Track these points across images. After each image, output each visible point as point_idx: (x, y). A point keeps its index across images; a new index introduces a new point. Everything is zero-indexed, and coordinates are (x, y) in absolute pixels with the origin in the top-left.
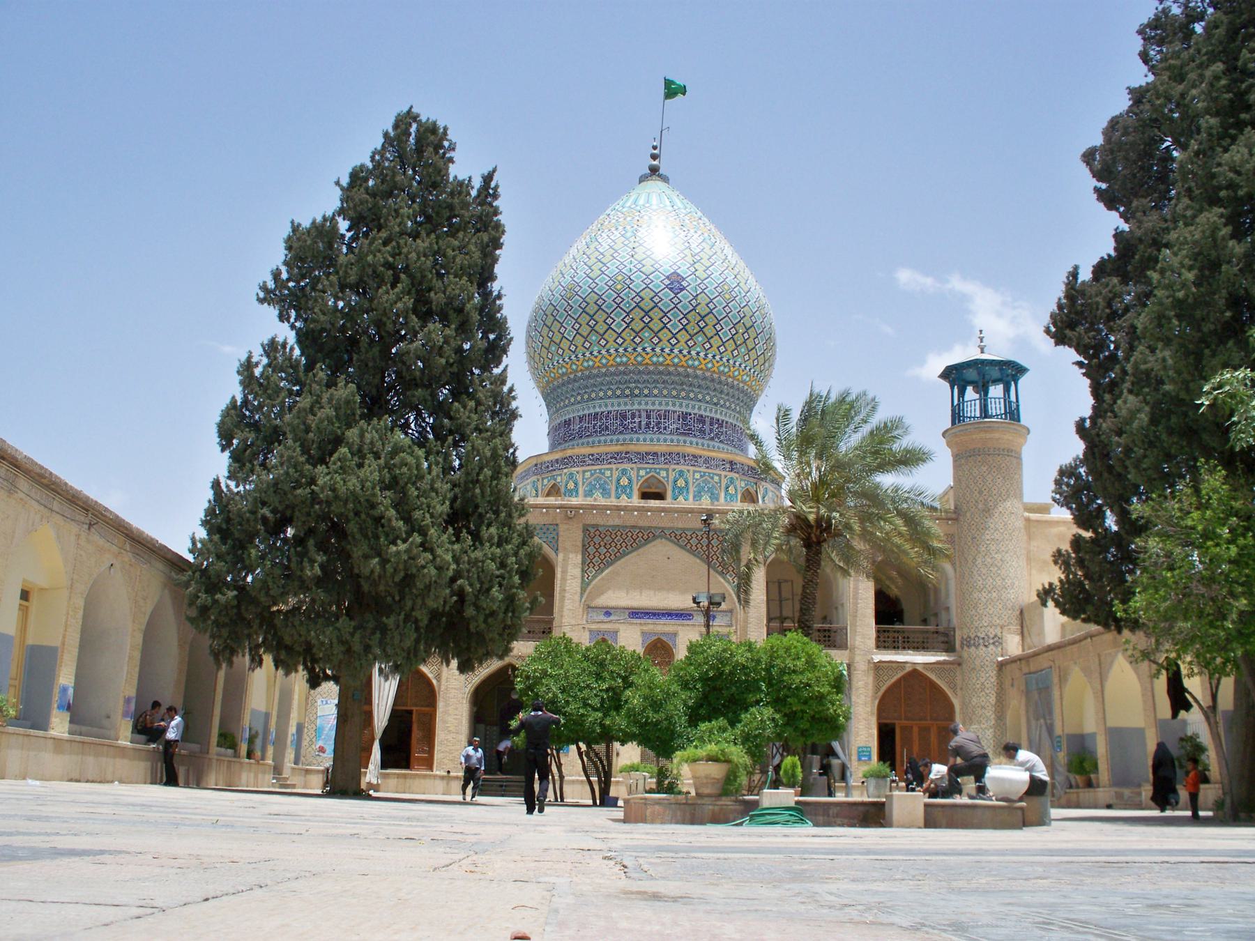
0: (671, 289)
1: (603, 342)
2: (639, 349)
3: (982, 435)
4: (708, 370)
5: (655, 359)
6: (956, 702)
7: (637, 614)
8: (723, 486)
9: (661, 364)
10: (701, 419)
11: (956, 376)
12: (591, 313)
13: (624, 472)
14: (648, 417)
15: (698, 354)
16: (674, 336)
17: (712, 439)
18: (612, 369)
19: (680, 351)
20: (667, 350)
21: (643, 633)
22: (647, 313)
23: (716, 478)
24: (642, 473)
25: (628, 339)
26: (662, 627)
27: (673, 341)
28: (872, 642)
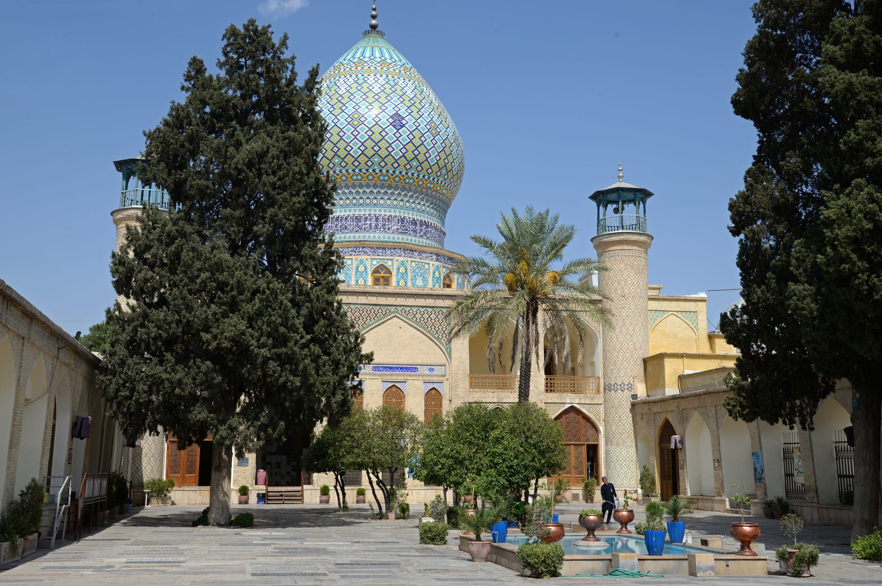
0: (394, 126)
1: (343, 164)
2: (371, 170)
6: (601, 429)
8: (431, 271)
10: (414, 222)
11: (601, 198)
12: (335, 142)
13: (361, 262)
14: (377, 219)
15: (413, 174)
16: (396, 161)
17: (422, 236)
19: (400, 173)
20: (391, 172)
22: (376, 144)
23: (427, 266)
24: (374, 262)
26: (397, 376)
27: (396, 165)
28: (542, 387)
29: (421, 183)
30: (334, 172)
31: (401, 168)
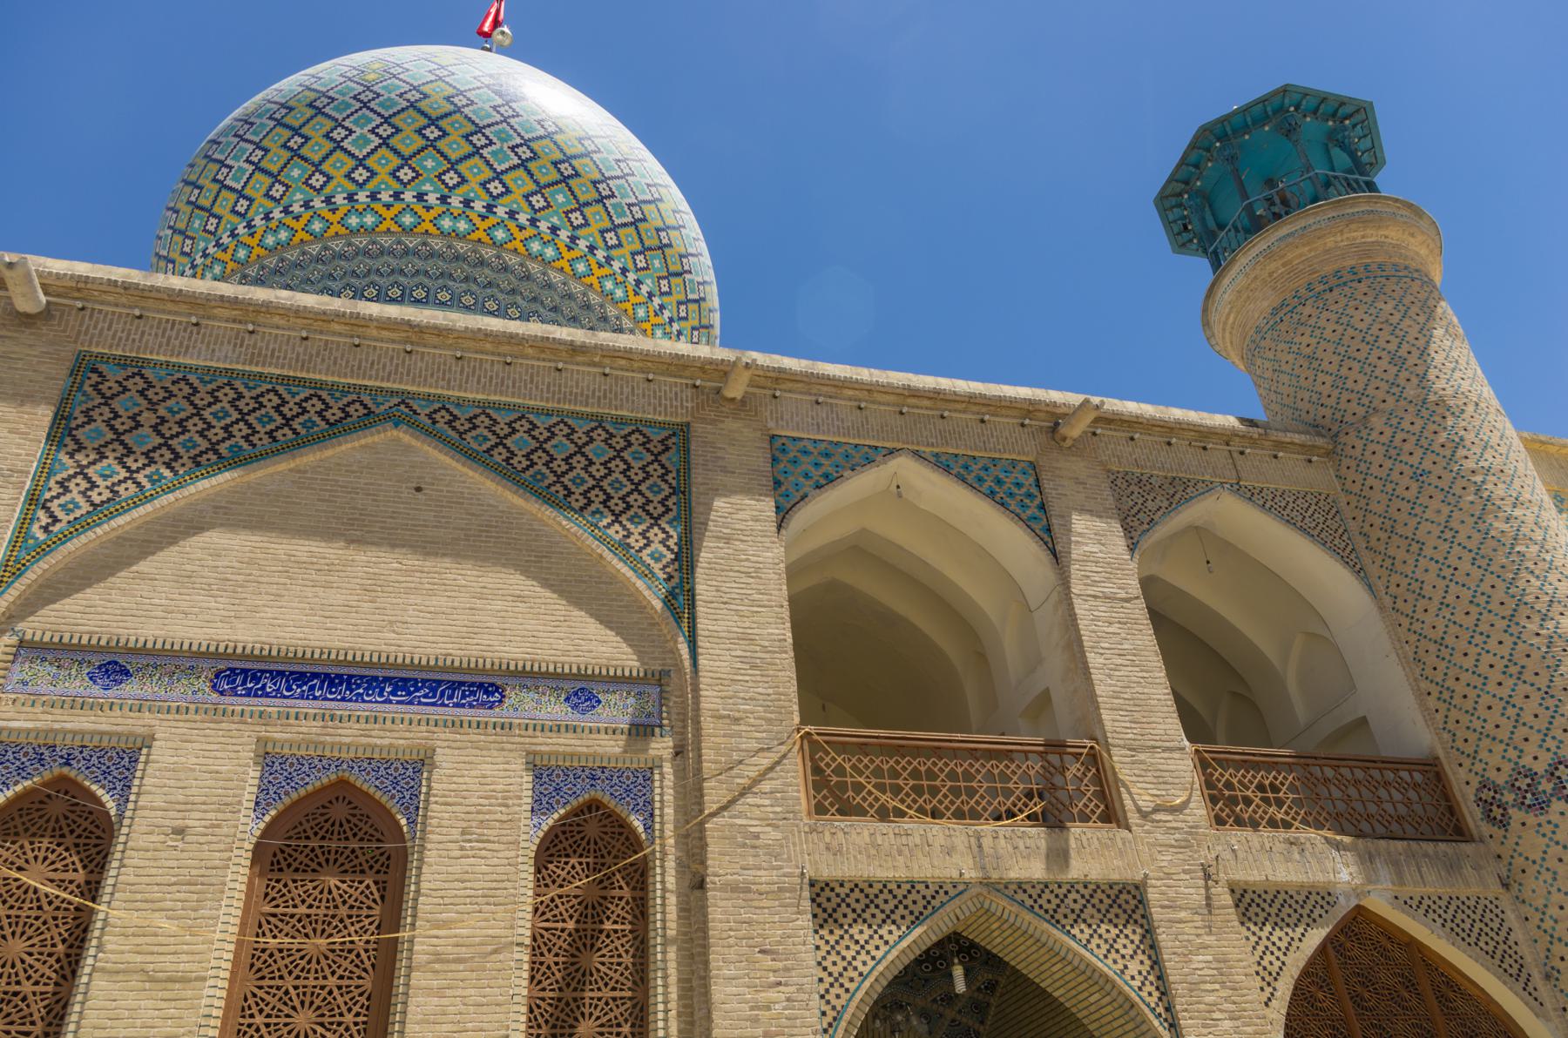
1: (317, 181)
2: (408, 196)
3: (1357, 234)
4: (578, 277)
5: (446, 223)
7: (245, 675)
9: (461, 237)
15: (554, 230)
16: (498, 176)
18: (338, 245)
19: (512, 214)
20: (478, 206)
21: (269, 759)
22: (433, 122)
29: (581, 267)
30: (286, 211)
31: (516, 200)
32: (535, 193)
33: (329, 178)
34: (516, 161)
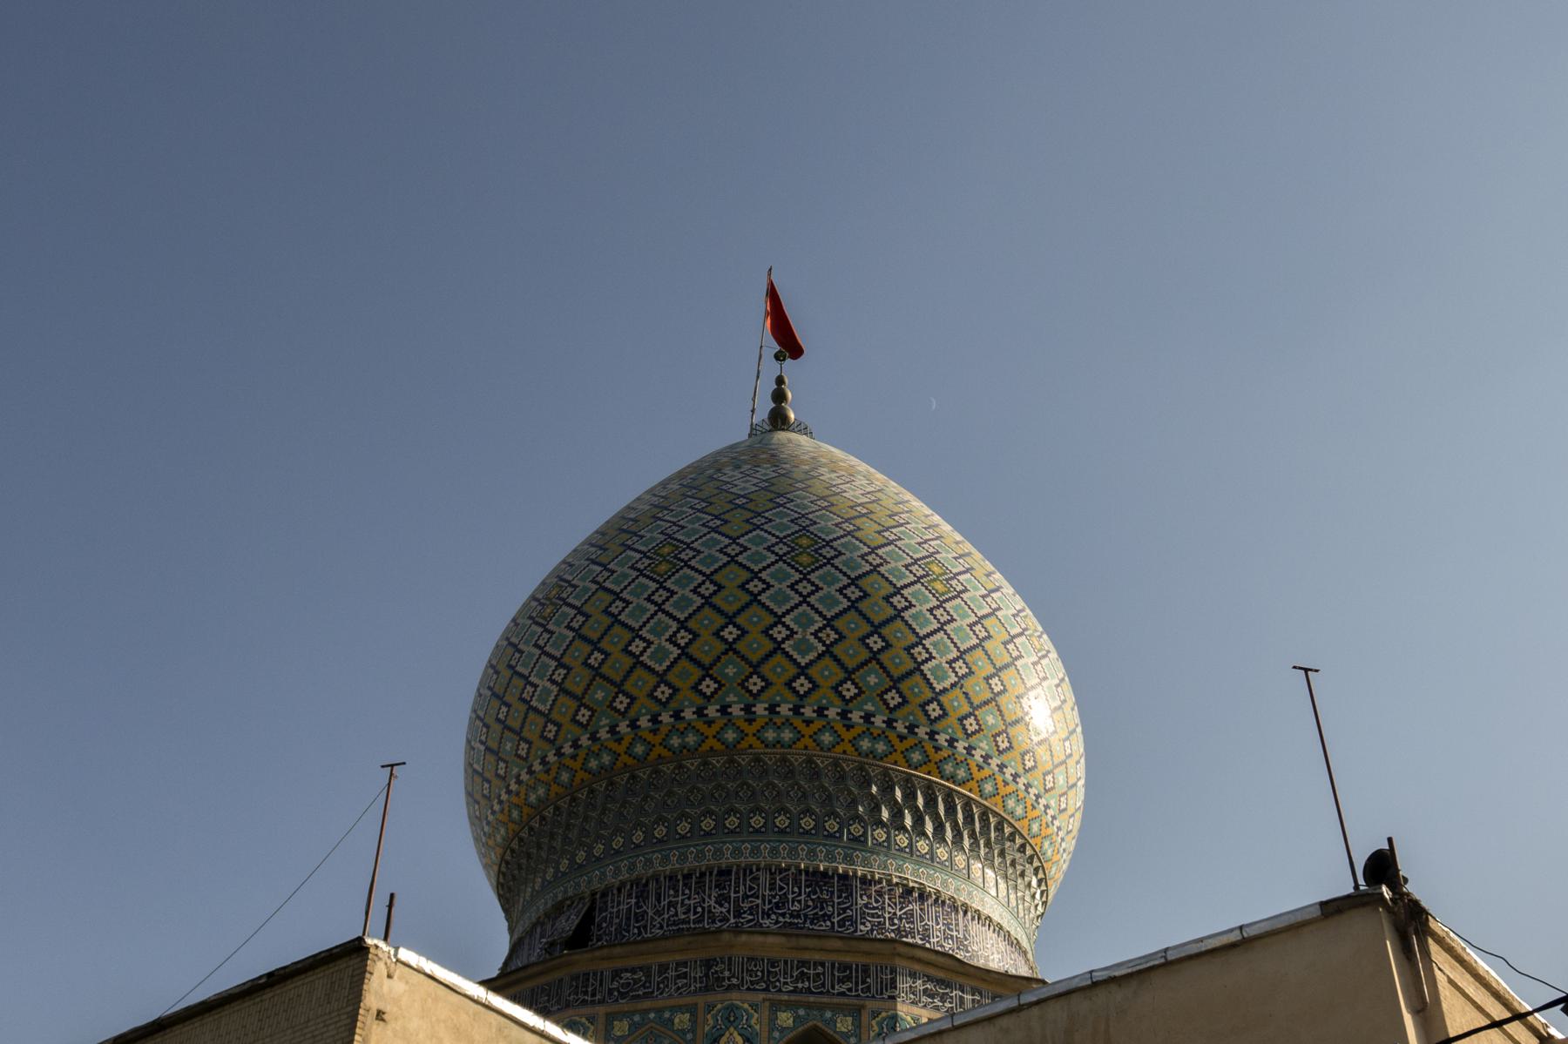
15: (867, 717)
16: (803, 671)
25: (684, 685)
31: (824, 695)
32: (857, 600)
33: (633, 699)
34: (821, 648)
